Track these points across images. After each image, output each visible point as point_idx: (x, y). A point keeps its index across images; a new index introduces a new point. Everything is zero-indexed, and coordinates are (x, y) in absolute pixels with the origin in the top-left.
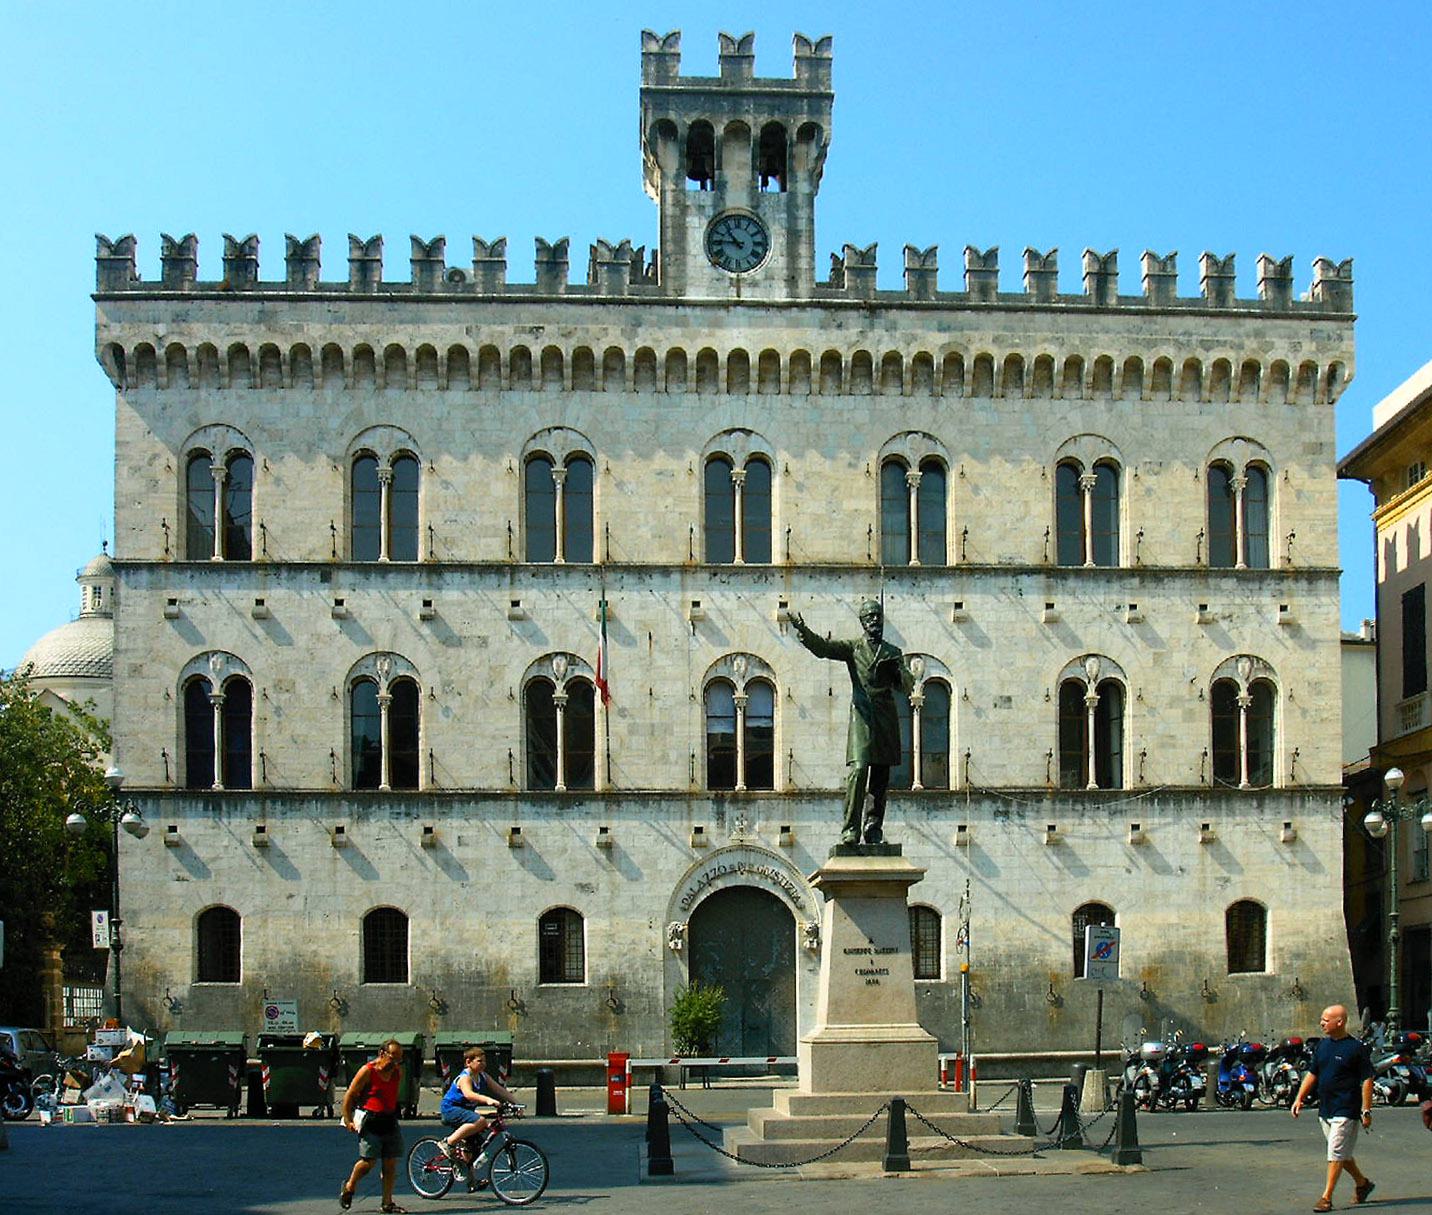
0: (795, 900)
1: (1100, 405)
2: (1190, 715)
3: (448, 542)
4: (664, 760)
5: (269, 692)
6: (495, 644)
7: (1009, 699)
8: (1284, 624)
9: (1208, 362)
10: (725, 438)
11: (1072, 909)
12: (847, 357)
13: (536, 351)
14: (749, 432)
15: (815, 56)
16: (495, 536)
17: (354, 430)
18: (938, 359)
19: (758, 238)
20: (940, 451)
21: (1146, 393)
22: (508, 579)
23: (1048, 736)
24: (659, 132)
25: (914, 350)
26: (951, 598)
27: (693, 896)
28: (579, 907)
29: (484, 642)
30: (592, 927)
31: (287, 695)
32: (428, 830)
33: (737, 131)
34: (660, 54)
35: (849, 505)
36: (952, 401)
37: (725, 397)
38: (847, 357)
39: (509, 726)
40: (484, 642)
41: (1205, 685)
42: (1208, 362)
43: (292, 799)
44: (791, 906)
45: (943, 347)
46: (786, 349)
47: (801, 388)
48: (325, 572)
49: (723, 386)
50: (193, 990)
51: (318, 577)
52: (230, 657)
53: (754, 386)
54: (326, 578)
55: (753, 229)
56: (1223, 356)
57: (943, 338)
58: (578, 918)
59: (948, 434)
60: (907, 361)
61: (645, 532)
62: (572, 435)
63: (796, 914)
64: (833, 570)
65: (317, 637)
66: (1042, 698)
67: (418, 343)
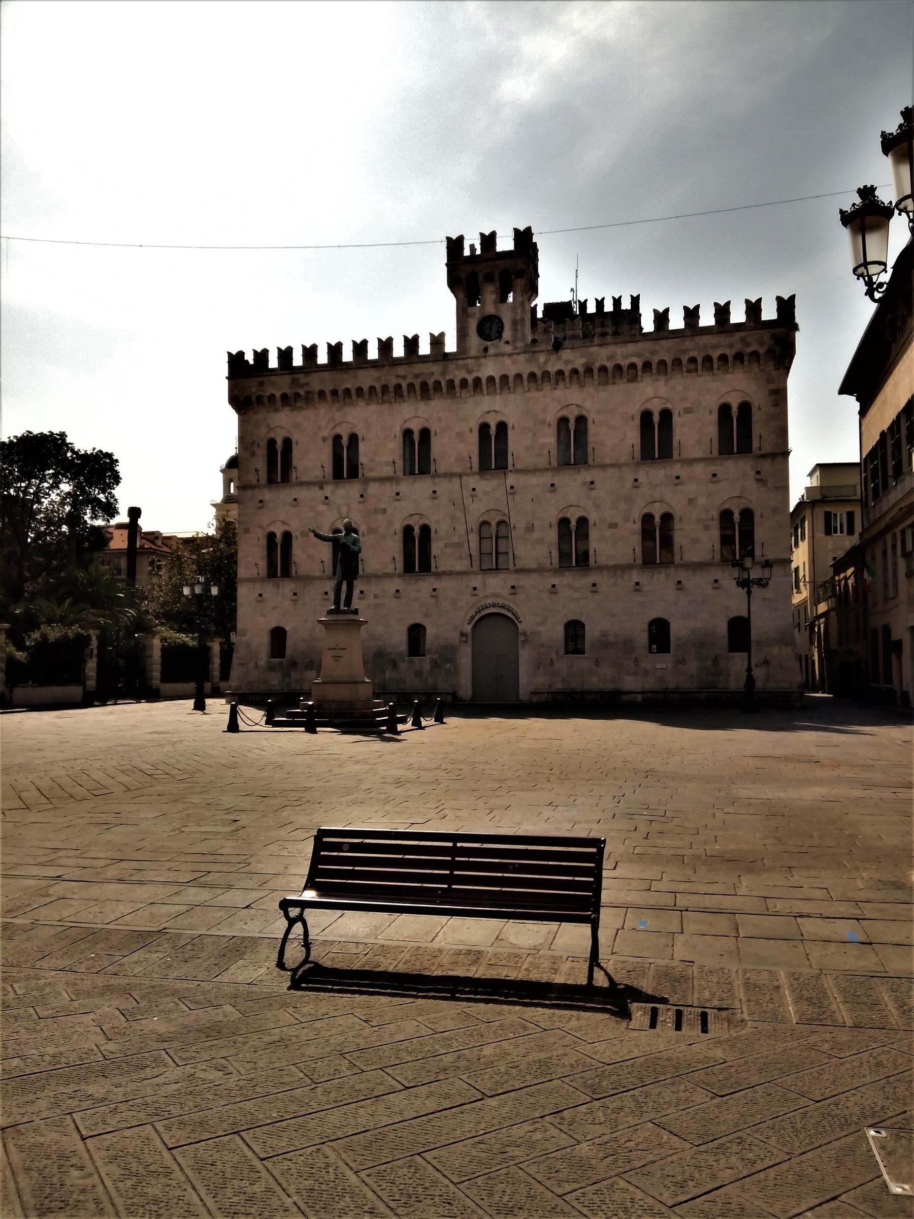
0: (517, 618)
1: (662, 383)
2: (706, 528)
3: (371, 470)
4: (460, 558)
5: (299, 537)
6: (389, 511)
7: (616, 524)
8: (758, 480)
9: (715, 355)
10: (487, 415)
11: (648, 621)
12: (539, 373)
13: (404, 385)
14: (497, 412)
15: (524, 238)
16: (388, 465)
17: (331, 425)
18: (581, 370)
19: (500, 325)
20: (584, 413)
21: (685, 374)
22: (394, 484)
23: (636, 540)
24: (453, 283)
25: (569, 368)
26: (589, 479)
27: (473, 618)
28: (424, 623)
29: (384, 511)
30: (430, 631)
31: (305, 538)
32: (362, 592)
33: (489, 278)
34: (455, 245)
35: (543, 440)
36: (589, 389)
37: (486, 397)
38: (539, 373)
39: (395, 546)
40: (384, 511)
41: (715, 514)
42: (715, 355)
43: (309, 579)
44: (516, 621)
45: (583, 365)
46: (512, 373)
47: (519, 390)
48: (321, 485)
49: (485, 392)
50: (268, 662)
51: (318, 488)
52: (284, 523)
53: (498, 391)
54: (321, 488)
55: (497, 321)
56: (722, 352)
57: (583, 361)
58: (424, 628)
59: (588, 404)
60: (567, 373)
61: (452, 459)
62: (421, 420)
63: (519, 625)
64: (535, 471)
65: (318, 513)
66: (632, 523)
67: (356, 386)
